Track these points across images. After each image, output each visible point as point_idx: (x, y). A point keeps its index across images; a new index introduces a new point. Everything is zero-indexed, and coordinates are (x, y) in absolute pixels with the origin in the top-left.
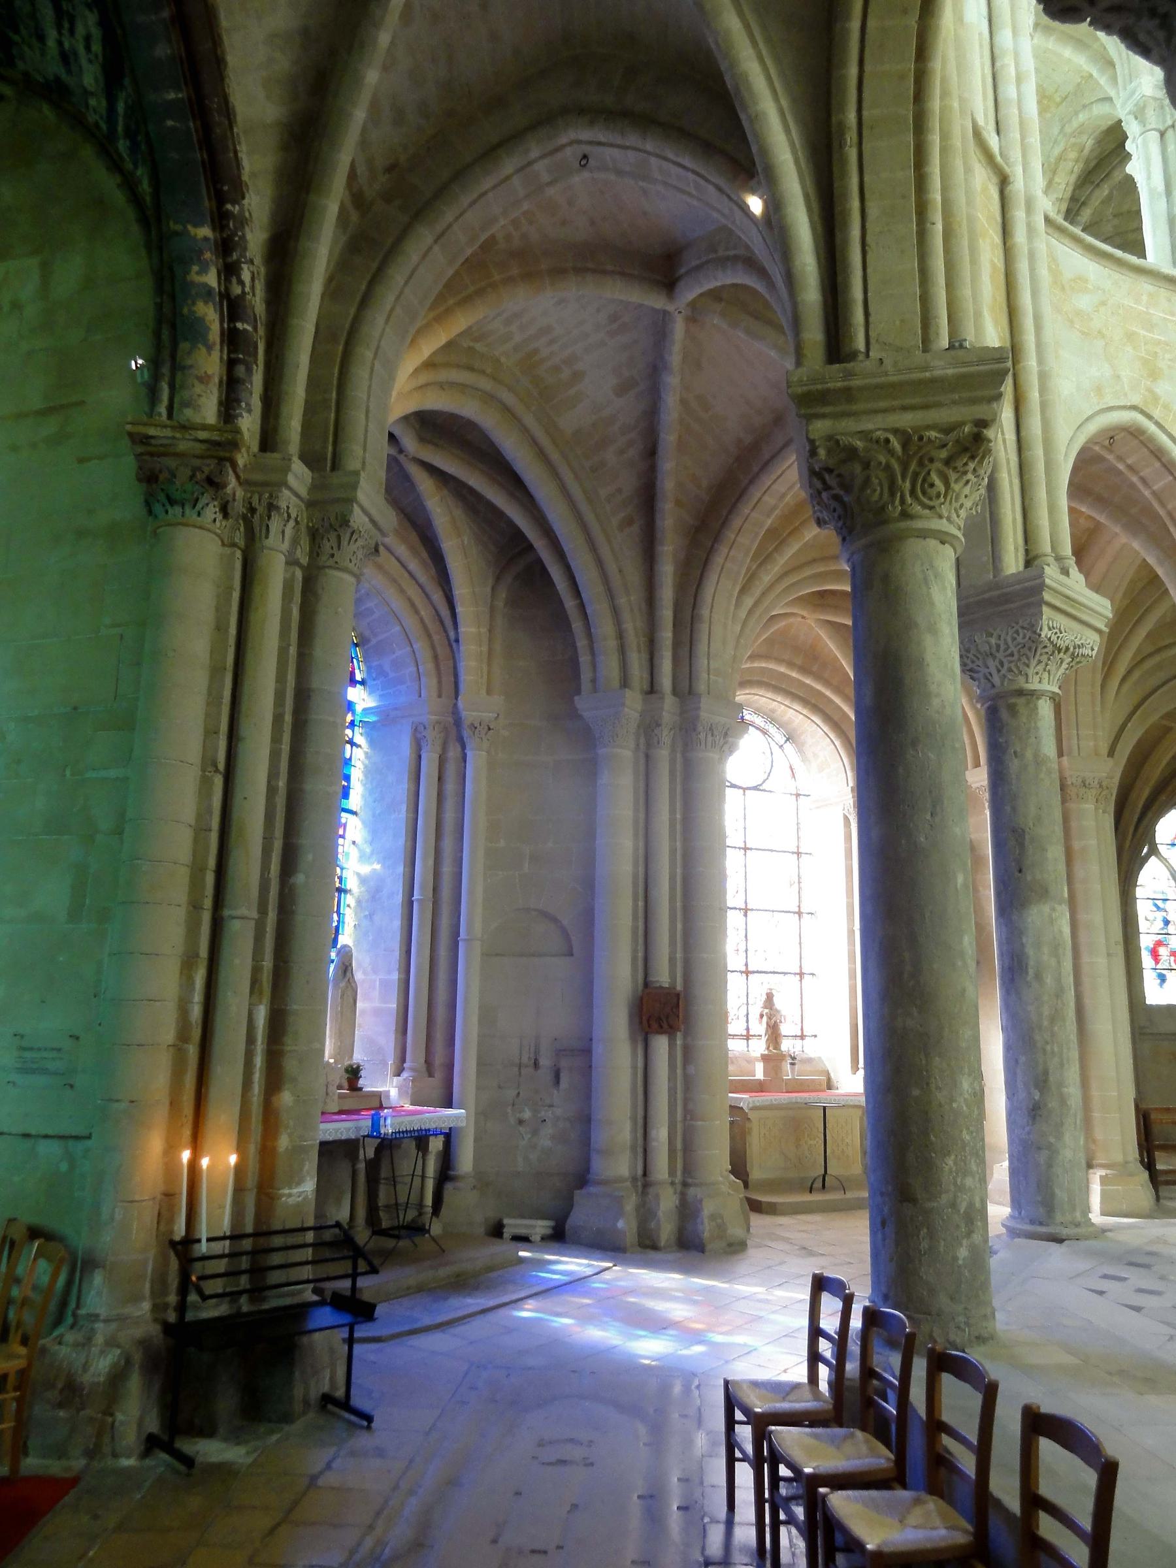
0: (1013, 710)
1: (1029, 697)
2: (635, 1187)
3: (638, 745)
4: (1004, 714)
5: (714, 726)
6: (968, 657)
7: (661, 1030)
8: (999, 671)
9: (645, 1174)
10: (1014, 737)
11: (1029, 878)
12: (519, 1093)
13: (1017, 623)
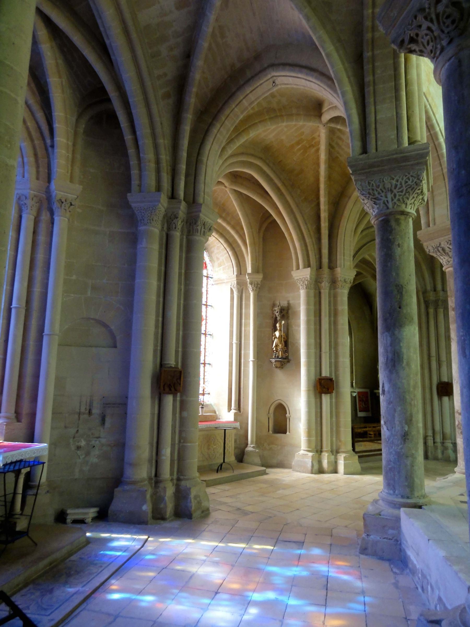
0: (398, 222)
1: (406, 216)
2: (151, 484)
3: (163, 228)
4: (393, 223)
5: (206, 223)
6: (377, 191)
8: (392, 200)
9: (156, 475)
10: (398, 236)
11: (405, 311)
12: (78, 430)
13: (409, 174)
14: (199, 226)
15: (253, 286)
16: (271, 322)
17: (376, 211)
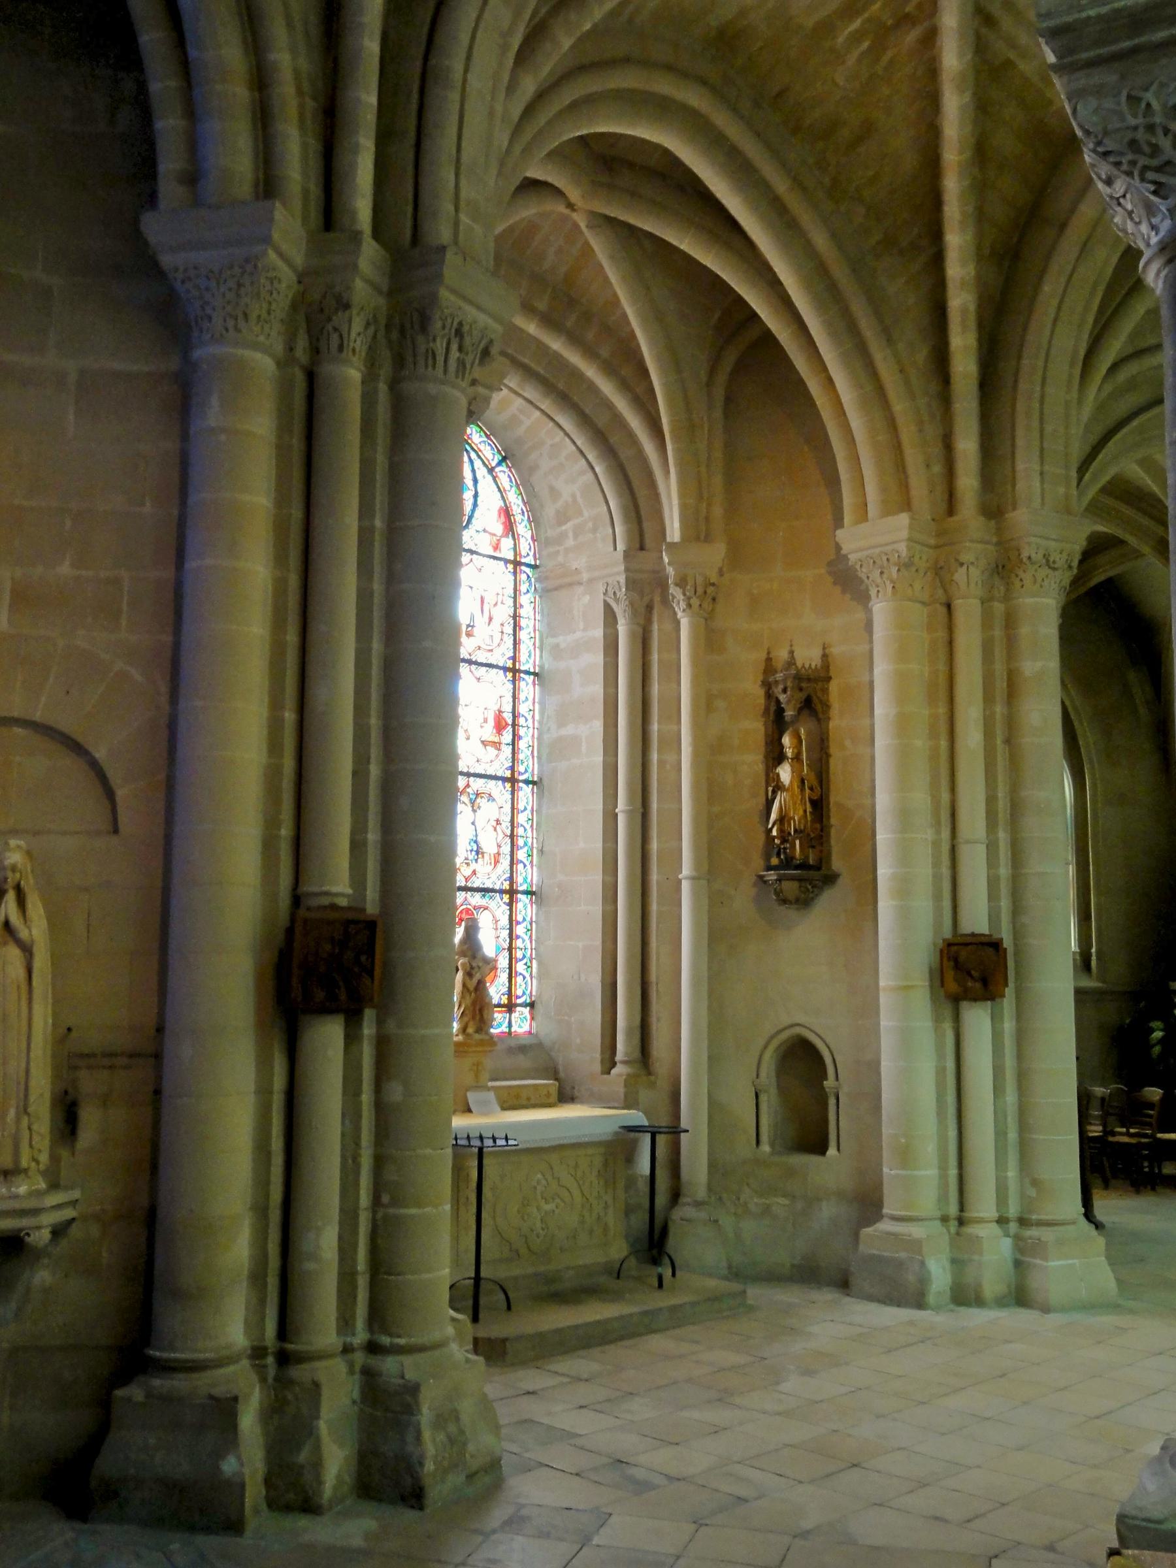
2: (261, 1370)
3: (291, 349)
5: (466, 328)
7: (326, 1009)
9: (283, 1333)
14: (438, 340)
15: (688, 594)
16: (755, 727)
17: (1166, 225)
